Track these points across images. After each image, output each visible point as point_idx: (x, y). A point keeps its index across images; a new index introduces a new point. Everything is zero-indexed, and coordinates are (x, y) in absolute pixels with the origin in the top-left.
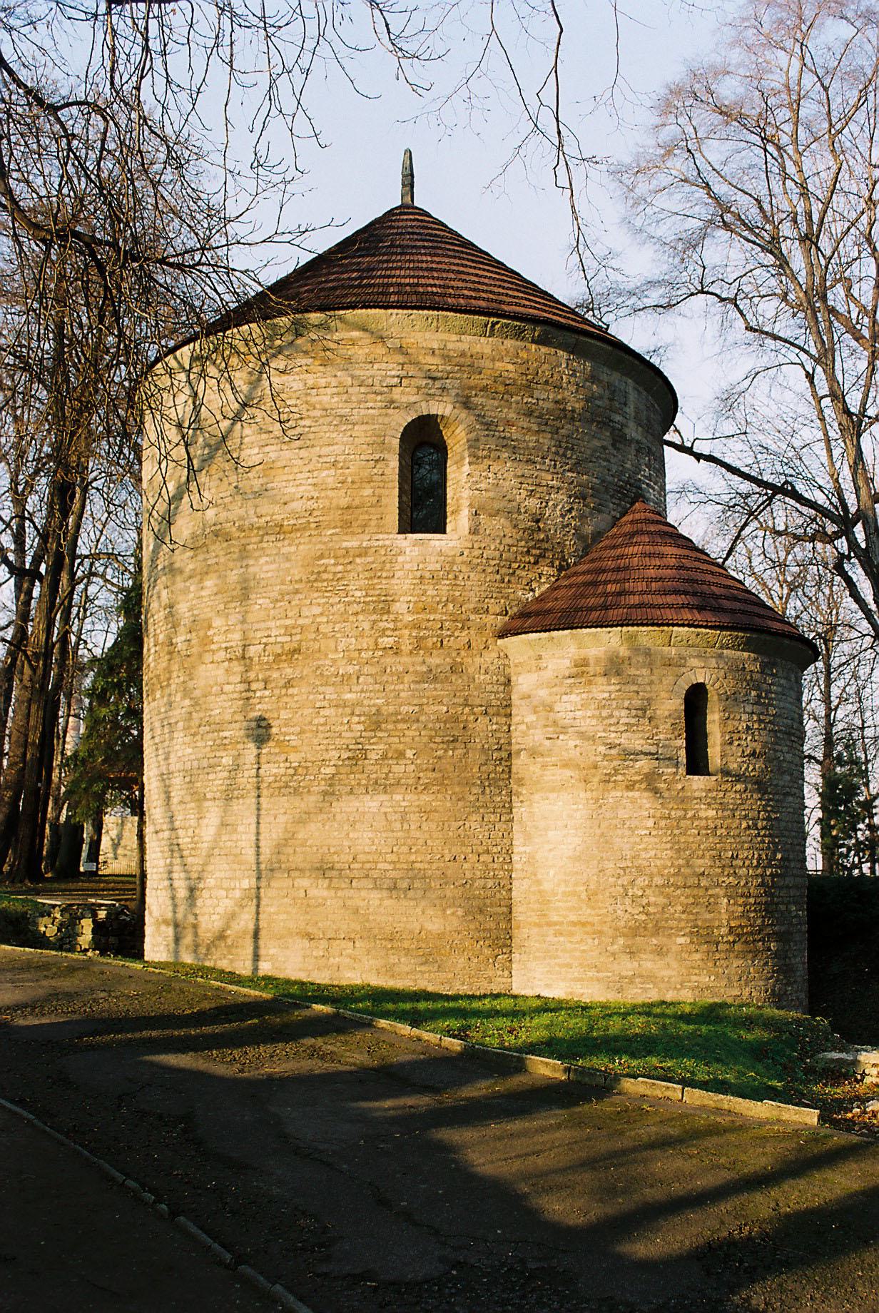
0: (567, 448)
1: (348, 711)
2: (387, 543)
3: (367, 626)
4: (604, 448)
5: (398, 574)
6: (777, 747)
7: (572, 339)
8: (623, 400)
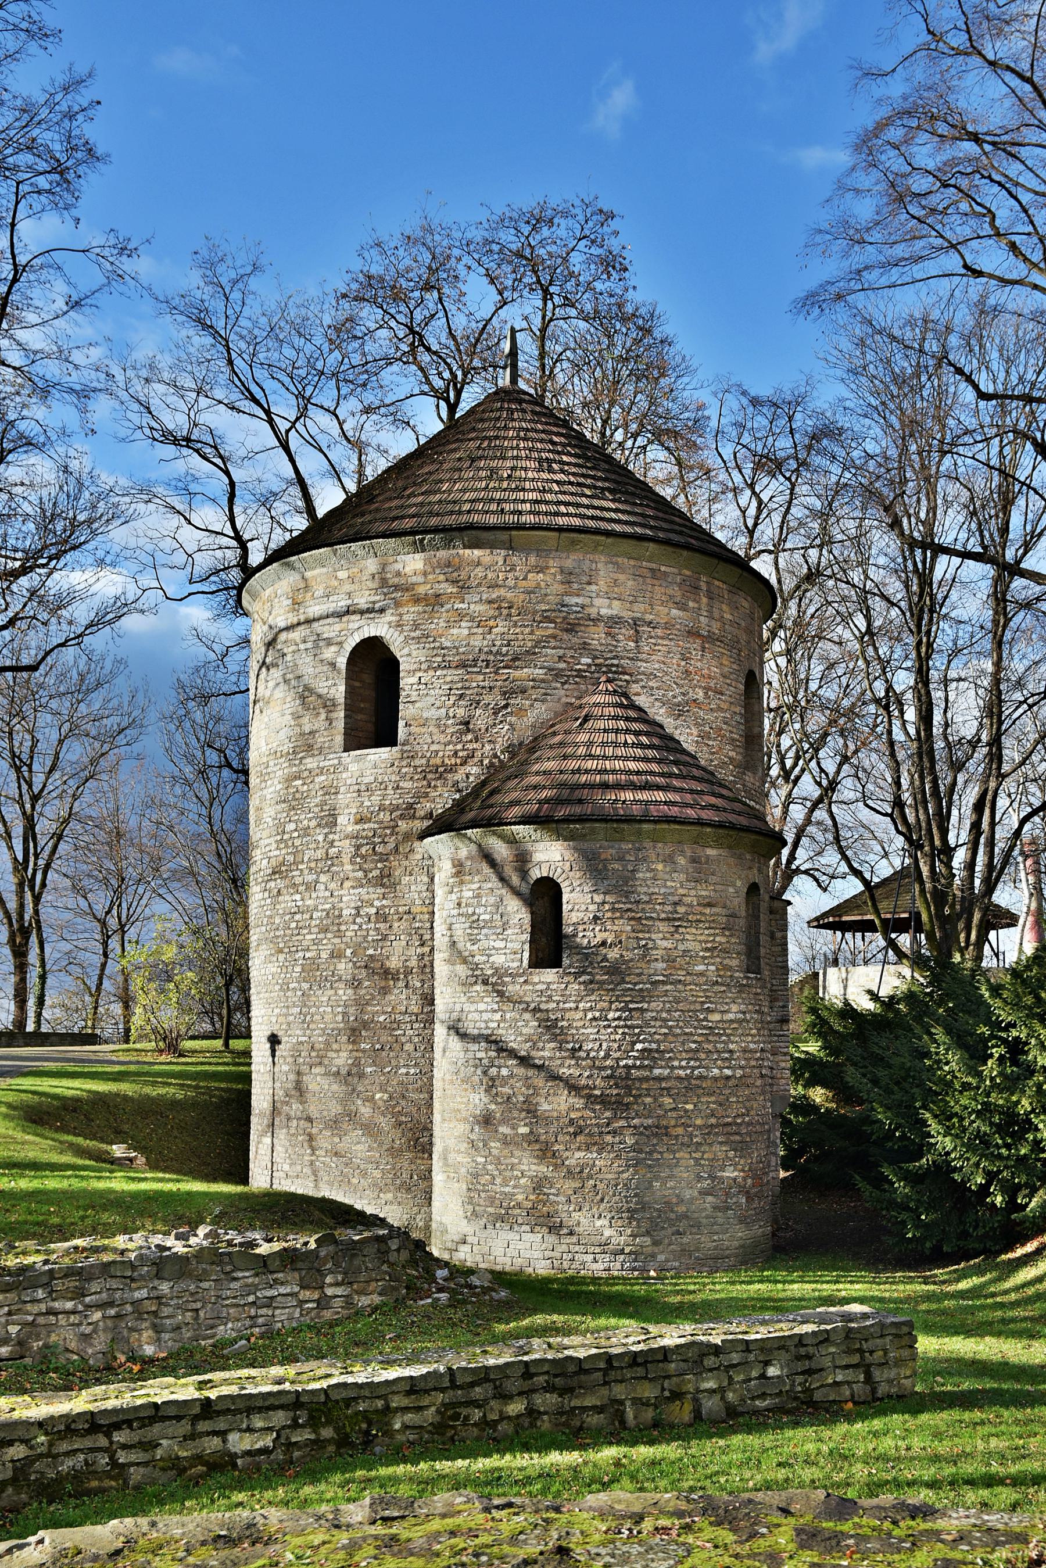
0: (502, 645)
1: (307, 916)
2: (336, 762)
3: (321, 838)
4: (554, 637)
5: (342, 789)
6: (641, 935)
7: (504, 536)
8: (585, 579)
